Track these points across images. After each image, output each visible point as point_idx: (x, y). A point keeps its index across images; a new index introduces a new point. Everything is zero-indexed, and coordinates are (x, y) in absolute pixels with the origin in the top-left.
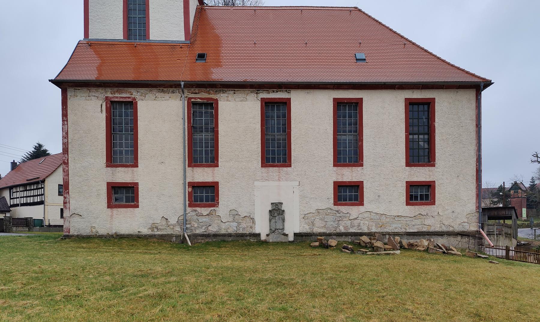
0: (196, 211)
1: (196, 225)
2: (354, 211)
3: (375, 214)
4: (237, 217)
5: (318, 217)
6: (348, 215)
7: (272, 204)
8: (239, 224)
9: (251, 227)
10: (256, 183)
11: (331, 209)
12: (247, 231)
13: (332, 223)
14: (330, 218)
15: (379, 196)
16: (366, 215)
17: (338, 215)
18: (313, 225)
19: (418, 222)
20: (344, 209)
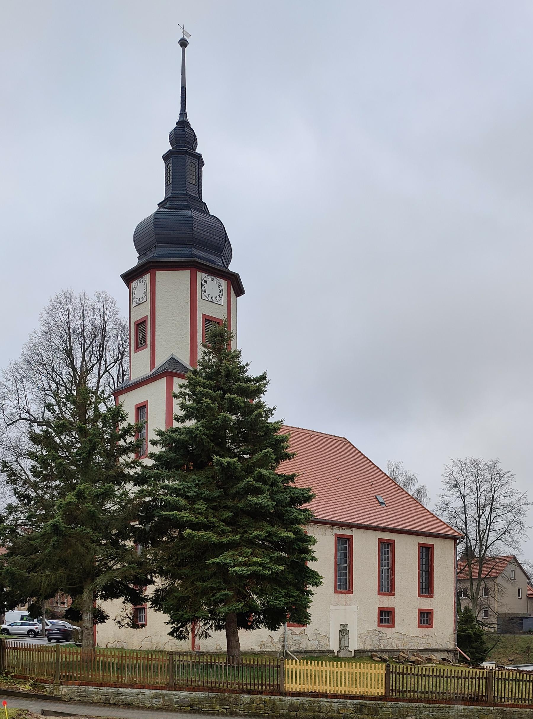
0: (291, 630)
1: (291, 643)
2: (388, 631)
3: (400, 635)
4: (318, 636)
5: (368, 637)
6: (385, 635)
7: (341, 625)
8: (319, 641)
9: (327, 645)
10: (332, 607)
11: (376, 630)
12: (325, 648)
13: (376, 641)
14: (375, 637)
15: (403, 620)
16: (396, 635)
17: (380, 635)
18: (365, 643)
19: (423, 641)
20: (383, 630)
